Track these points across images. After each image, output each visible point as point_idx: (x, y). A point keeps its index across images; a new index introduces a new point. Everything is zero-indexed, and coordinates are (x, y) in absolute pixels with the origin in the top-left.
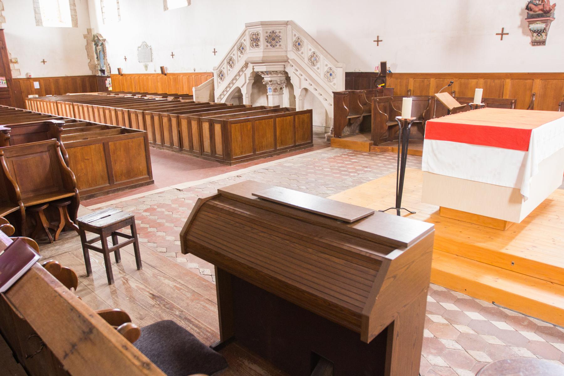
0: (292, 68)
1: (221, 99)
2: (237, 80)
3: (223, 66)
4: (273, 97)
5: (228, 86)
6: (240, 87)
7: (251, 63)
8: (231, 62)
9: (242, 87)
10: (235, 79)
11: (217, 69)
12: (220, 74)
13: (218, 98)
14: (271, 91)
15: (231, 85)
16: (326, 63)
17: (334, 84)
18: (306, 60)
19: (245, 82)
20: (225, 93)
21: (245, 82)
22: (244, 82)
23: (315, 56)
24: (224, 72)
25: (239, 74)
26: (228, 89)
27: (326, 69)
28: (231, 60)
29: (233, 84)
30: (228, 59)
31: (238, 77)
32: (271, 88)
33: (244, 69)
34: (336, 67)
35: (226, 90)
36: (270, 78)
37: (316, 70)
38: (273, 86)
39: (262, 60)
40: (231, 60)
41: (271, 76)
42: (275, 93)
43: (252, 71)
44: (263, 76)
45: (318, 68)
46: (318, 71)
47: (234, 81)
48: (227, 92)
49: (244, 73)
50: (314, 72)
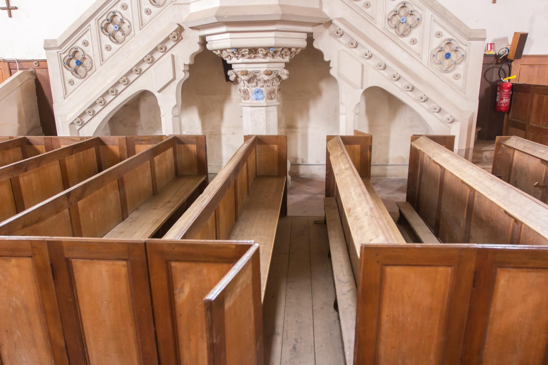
0: (339, 41)
1: (83, 125)
2: (140, 73)
3: (84, 38)
4: (266, 112)
5: (113, 90)
6: (154, 90)
7: (192, 28)
8: (111, 28)
9: (159, 91)
10: (137, 70)
11: (61, 47)
12: (71, 59)
13: (72, 123)
14: (260, 96)
15: (120, 88)
16: (438, 29)
17: (457, 76)
18: (381, 20)
19: (174, 79)
20: (97, 108)
21: (174, 79)
22: (172, 77)
23: (402, 13)
24: (85, 52)
25: (150, 59)
26: (109, 98)
27: (437, 42)
28: (112, 21)
29: (128, 84)
30: (104, 18)
31: (144, 66)
32: (263, 89)
33: (169, 45)
34: (470, 39)
35: (102, 101)
36: (265, 65)
37: (409, 45)
38: (269, 84)
39: (283, 15)
40: (111, 21)
41: (272, 60)
42: (271, 101)
43: (196, 48)
44: (229, 62)
45: (414, 42)
46: (413, 47)
47: (132, 78)
48: (105, 105)
49: (168, 54)
50: (404, 50)
